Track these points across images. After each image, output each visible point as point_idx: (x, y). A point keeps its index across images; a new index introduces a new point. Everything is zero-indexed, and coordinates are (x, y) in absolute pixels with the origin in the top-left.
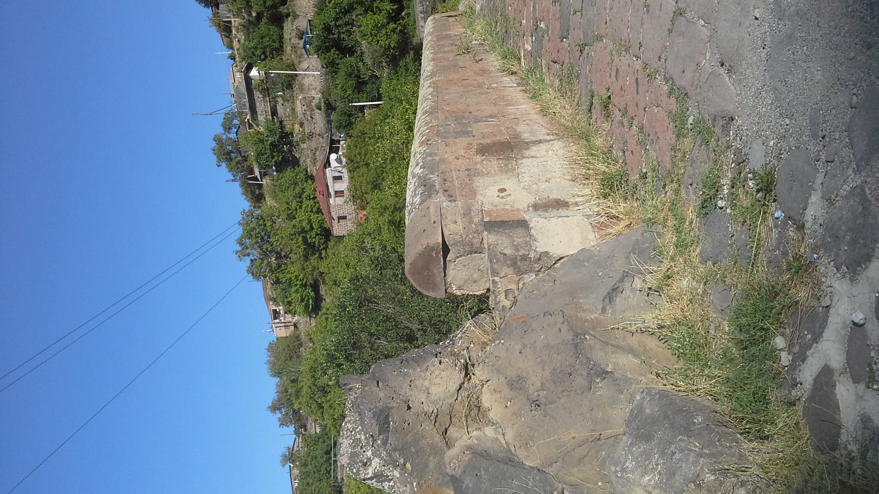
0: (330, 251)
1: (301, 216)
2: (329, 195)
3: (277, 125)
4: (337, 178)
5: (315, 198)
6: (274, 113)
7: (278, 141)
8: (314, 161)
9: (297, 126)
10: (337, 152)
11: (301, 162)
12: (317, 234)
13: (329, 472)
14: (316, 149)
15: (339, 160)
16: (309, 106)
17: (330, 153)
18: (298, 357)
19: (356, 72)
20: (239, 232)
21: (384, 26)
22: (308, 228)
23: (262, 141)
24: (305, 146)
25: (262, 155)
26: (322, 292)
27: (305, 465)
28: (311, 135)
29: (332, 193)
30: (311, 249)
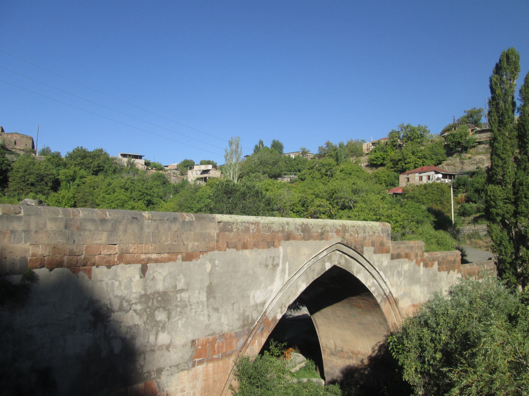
0: (393, 173)
1: (413, 158)
2: (420, 173)
3: (472, 145)
4: (429, 177)
5: (423, 165)
6: (480, 143)
7: (462, 145)
8: (448, 165)
9: (469, 155)
10: (443, 178)
11: (450, 158)
12: (403, 166)
13: (290, 171)
14: (455, 166)
15: (438, 179)
16: (479, 162)
17: (442, 174)
18: (352, 156)
20: (415, 125)
22: (406, 162)
23: (461, 137)
24: (458, 160)
25: (453, 137)
26: (380, 168)
27: (295, 159)
28: (462, 163)
29: (421, 175)
30: (395, 163)
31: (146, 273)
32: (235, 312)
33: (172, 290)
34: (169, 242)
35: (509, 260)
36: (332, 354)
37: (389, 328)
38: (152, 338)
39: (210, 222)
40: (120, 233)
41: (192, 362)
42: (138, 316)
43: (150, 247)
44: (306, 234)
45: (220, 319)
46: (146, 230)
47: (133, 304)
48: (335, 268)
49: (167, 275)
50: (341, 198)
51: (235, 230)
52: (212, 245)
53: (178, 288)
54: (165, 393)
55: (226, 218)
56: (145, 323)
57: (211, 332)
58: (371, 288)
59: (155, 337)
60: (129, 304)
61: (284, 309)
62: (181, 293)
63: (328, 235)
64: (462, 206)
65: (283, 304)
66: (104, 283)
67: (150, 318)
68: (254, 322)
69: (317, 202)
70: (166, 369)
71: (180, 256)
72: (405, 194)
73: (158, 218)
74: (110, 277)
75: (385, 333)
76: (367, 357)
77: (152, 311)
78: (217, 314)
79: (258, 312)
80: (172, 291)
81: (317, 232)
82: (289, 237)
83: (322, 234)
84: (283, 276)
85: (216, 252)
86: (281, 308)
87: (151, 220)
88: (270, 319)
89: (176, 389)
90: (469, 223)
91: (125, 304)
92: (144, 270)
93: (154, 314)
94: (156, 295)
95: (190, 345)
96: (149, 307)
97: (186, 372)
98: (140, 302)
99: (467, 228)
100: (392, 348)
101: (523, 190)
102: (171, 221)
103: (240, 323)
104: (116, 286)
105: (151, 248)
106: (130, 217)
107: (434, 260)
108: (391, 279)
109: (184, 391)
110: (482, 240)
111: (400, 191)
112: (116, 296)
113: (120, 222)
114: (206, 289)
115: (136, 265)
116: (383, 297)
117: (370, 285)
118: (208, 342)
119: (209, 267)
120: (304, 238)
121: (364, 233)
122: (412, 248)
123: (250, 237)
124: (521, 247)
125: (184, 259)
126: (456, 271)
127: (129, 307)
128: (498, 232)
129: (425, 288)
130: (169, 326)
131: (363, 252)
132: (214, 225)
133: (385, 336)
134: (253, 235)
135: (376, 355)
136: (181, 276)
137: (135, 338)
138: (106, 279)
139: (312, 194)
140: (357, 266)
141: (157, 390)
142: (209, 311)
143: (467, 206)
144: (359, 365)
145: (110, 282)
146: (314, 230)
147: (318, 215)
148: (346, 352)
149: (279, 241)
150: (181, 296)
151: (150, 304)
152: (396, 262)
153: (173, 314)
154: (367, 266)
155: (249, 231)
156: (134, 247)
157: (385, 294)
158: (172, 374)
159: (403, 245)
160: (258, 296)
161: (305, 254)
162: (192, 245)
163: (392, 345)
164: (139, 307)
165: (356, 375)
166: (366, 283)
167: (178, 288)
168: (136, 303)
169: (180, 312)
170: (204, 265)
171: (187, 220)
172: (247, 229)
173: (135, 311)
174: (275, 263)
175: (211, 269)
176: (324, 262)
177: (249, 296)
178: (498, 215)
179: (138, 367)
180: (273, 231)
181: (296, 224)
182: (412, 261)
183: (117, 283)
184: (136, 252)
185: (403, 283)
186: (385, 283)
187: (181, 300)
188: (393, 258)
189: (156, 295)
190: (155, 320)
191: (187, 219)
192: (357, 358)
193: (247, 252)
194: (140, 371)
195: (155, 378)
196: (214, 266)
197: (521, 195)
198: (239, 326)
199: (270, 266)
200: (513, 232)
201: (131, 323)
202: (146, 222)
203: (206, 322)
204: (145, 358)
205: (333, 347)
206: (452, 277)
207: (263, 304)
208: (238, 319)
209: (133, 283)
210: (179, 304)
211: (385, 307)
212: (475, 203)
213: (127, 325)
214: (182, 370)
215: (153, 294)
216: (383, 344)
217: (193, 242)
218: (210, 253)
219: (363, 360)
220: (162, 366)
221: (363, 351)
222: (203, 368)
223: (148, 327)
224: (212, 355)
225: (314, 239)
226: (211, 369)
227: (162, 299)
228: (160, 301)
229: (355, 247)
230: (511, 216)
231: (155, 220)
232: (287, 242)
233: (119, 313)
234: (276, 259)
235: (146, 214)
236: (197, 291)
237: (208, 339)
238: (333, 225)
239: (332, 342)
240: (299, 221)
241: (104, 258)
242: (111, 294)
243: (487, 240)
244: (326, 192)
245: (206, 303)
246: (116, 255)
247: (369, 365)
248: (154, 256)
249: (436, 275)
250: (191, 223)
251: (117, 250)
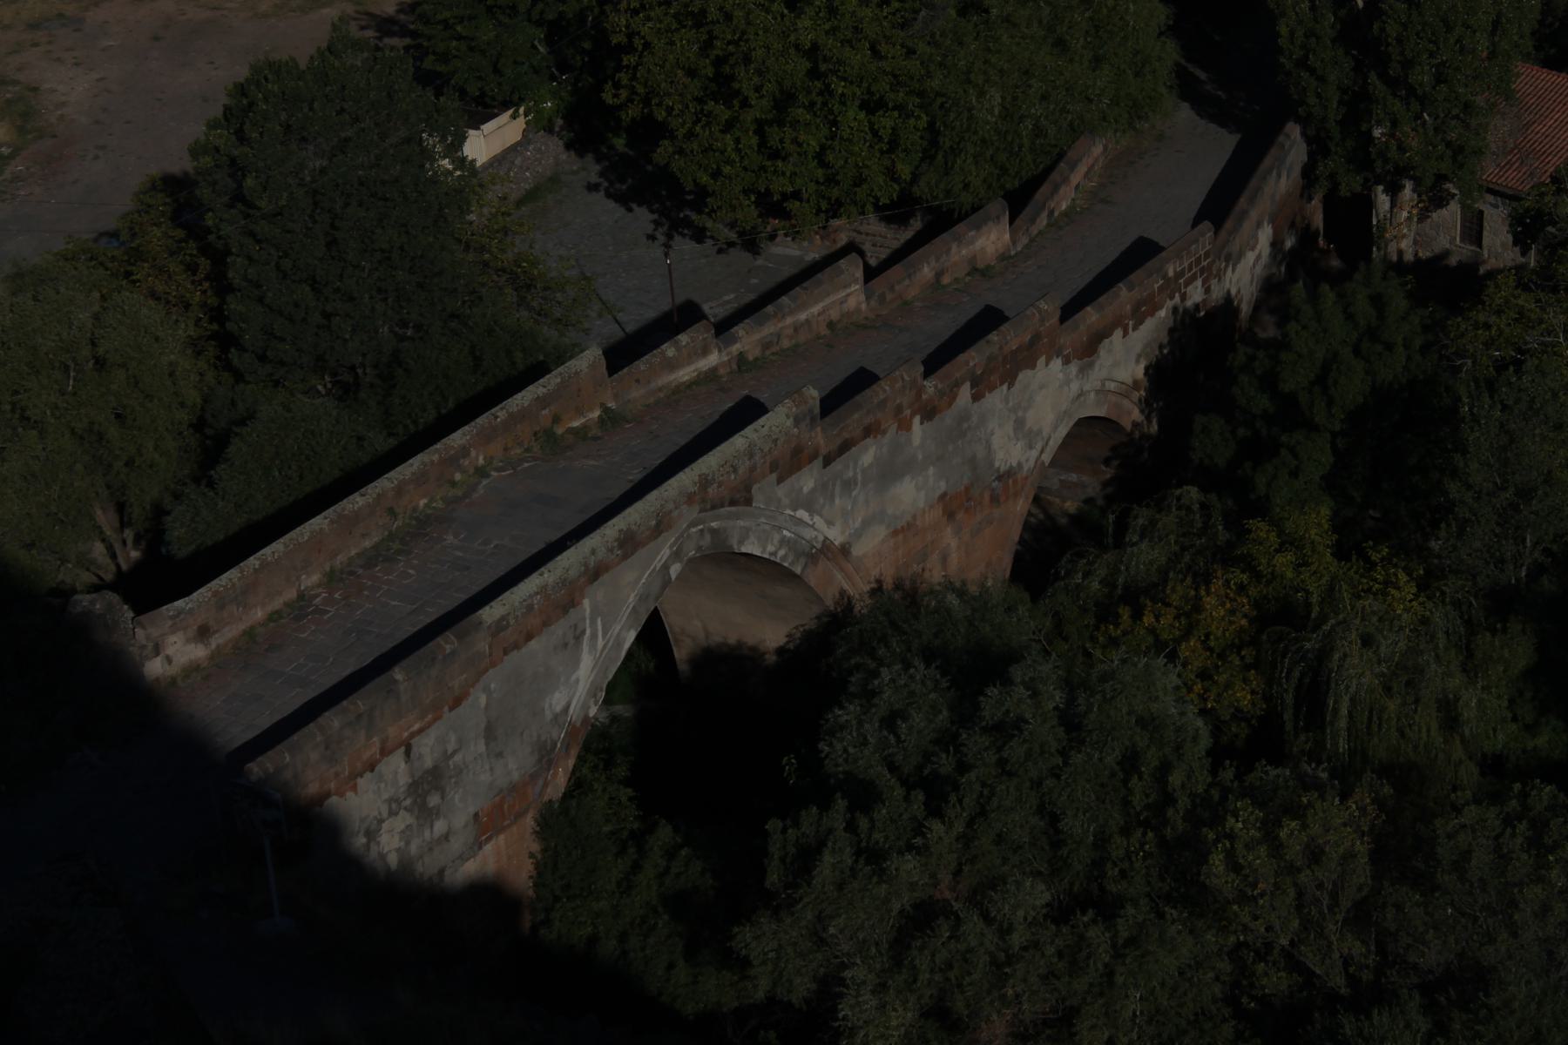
44: (629, 544)
82: (595, 573)
83: (658, 524)
84: (593, 646)
107: (958, 384)
119: (483, 700)
120: (625, 557)
125: (451, 709)
152: (837, 466)
160: (557, 700)
166: (764, 551)
172: (530, 608)
188: (828, 461)
191: (448, 648)
193: (533, 642)
199: (572, 641)
248: (416, 727)
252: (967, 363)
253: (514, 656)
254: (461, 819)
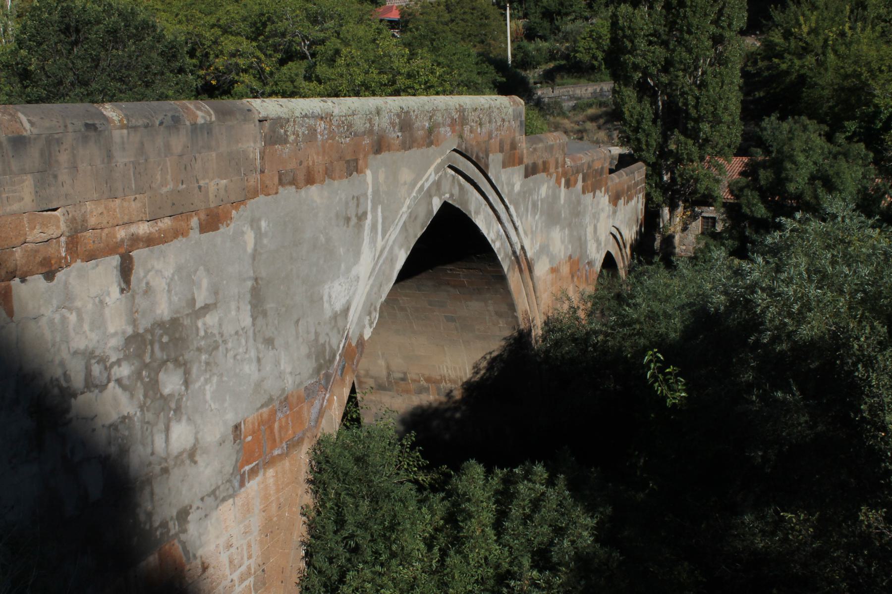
19: (564, 11)
21: (598, 43)
31: (133, 278)
32: (301, 340)
33: (187, 312)
34: (170, 186)
35: (652, 159)
36: (381, 388)
37: (517, 322)
38: (159, 442)
39: (245, 120)
40: (64, 176)
41: (238, 477)
42: (127, 393)
43: (134, 205)
45: (277, 363)
46: (122, 159)
47: (113, 364)
48: (446, 206)
49: (173, 275)
50: (283, 35)
51: (292, 138)
52: (252, 182)
53: (198, 306)
54: (198, 561)
55: (269, 107)
56: (142, 407)
57: (266, 397)
58: (494, 242)
59: (164, 436)
60: (106, 368)
61: (373, 317)
62: (205, 316)
63: (439, 132)
64: (519, 47)
65: (372, 304)
66: (44, 321)
67: (151, 393)
68: (334, 356)
69: (229, 44)
70: (194, 507)
71: (194, 222)
72: (407, 22)
73: (140, 122)
74: (55, 302)
75: (507, 333)
76: (460, 383)
77: (153, 375)
78: (271, 353)
79: (339, 332)
80: (188, 315)
81: (423, 128)
82: (380, 146)
83: (430, 131)
84: (373, 241)
85: (261, 198)
86: (370, 314)
87: (127, 127)
88: (354, 344)
89: (217, 546)
90: (535, 83)
91: (96, 369)
92: (126, 271)
93: (157, 381)
94: (158, 332)
95: (231, 437)
96: (146, 366)
97: (231, 501)
98: (126, 358)
99: (544, 92)
100: (653, 375)
101: (685, 17)
102: (168, 127)
103: (311, 365)
104: (71, 327)
105: (134, 206)
106: (79, 124)
107: (578, 172)
108: (524, 219)
109: (231, 546)
110: (568, 118)
111: (395, 16)
112: (76, 353)
113: (59, 142)
114: (248, 297)
115: (108, 258)
116: (510, 258)
117: (494, 238)
118: (261, 422)
119: (250, 238)
121: (490, 122)
122: (551, 147)
123: (318, 154)
124: (676, 131)
125: (205, 228)
126: (603, 189)
127: (106, 375)
128: (634, 102)
129: (567, 231)
130: (189, 404)
131: (487, 166)
132: (251, 128)
133: (505, 339)
134: (323, 146)
135: (482, 377)
136: (201, 271)
137: (127, 451)
138: (48, 312)
139: (213, 26)
140: (476, 198)
141: (184, 559)
142: (257, 349)
143: (531, 47)
144: (441, 403)
145: (57, 317)
146: (418, 124)
147: (233, 75)
148: (414, 381)
149: (365, 156)
150: (204, 324)
151: (148, 360)
153: (194, 371)
154: (492, 196)
155: (316, 135)
156: (101, 209)
157: (514, 252)
158: (206, 516)
159: (540, 145)
161: (405, 183)
162: (216, 186)
163: (654, 369)
164: (124, 371)
165: (435, 423)
166: (488, 234)
167: (199, 305)
168: (118, 362)
169: (207, 364)
170: (243, 234)
171: (200, 121)
172: (313, 131)
173: (119, 381)
174: (360, 212)
175: (255, 244)
176: (431, 197)
177: (322, 298)
178: (636, 67)
179: (142, 517)
180: (355, 135)
181: (391, 111)
182: (551, 175)
183: (73, 318)
184: (105, 222)
185: (540, 225)
186: (516, 229)
187: (206, 332)
188: (526, 176)
189: (158, 332)
190: (161, 394)
192: (438, 389)
193: (314, 189)
194: (148, 527)
195: (176, 535)
196: (259, 235)
197: (682, 27)
198: (311, 371)
199: (354, 220)
200: (660, 103)
201: (114, 417)
202: (117, 133)
203: (256, 376)
204: (152, 494)
205: (384, 373)
206: (598, 203)
207: (346, 310)
208: (309, 356)
209: (107, 311)
210: (203, 343)
211: (514, 279)
212: (544, 38)
213: (108, 422)
214: (224, 500)
215: (150, 331)
216: (500, 356)
217: (217, 180)
218: (251, 203)
219: (451, 391)
220: (187, 502)
221: (453, 375)
222: (258, 484)
223: (149, 416)
224: (272, 449)
225: (420, 146)
226: (271, 481)
227: (170, 341)
228: (164, 344)
229: (477, 157)
230: (658, 71)
231: (135, 128)
232: (379, 156)
233: (89, 396)
234: (362, 200)
235: (110, 111)
236: (233, 305)
237: (261, 415)
238: (446, 110)
239: (382, 363)
240: (394, 103)
241: (37, 251)
242: (64, 347)
243: (576, 119)
244: (244, 19)
245: (252, 331)
246: (63, 239)
247: (464, 400)
248: (143, 229)
249: (579, 202)
250: (208, 128)
251: (63, 227)
252: (581, 159)
253: (288, 192)
254: (214, 431)
